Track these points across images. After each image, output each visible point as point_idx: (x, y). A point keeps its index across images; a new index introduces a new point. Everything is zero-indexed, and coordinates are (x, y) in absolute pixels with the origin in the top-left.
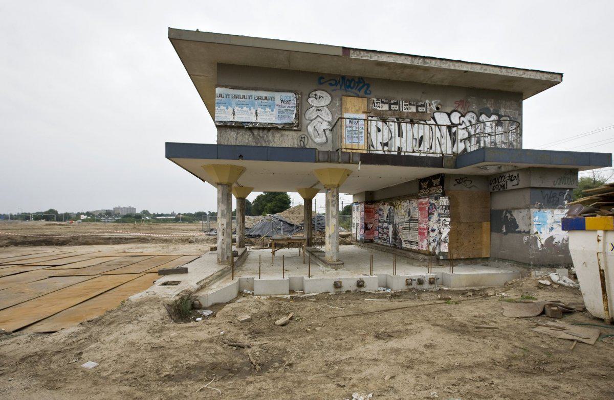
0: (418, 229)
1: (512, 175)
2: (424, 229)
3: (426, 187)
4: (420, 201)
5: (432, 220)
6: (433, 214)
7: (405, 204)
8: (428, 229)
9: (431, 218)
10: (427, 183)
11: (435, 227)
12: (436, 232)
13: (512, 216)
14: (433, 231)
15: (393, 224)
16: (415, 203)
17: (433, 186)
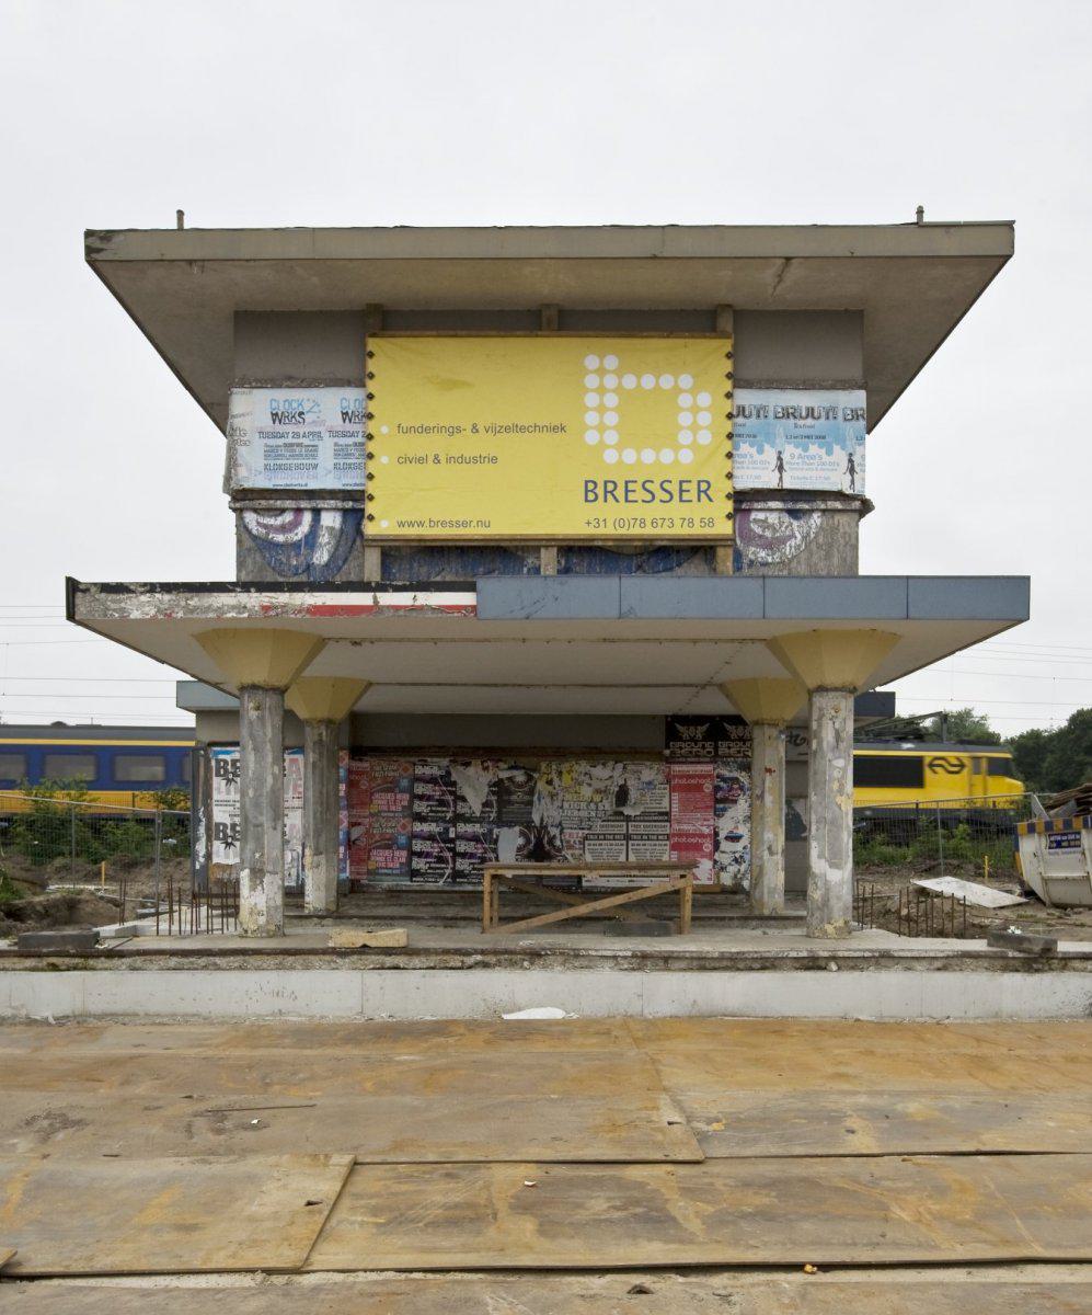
0: (668, 837)
1: (798, 736)
2: (702, 836)
3: (699, 736)
4: (677, 768)
5: (729, 814)
6: (735, 802)
7: (600, 772)
8: (716, 834)
9: (725, 810)
10: (705, 728)
11: (743, 830)
12: (745, 842)
13: (793, 809)
14: (734, 838)
15: (528, 824)
16: (650, 772)
17: (726, 737)
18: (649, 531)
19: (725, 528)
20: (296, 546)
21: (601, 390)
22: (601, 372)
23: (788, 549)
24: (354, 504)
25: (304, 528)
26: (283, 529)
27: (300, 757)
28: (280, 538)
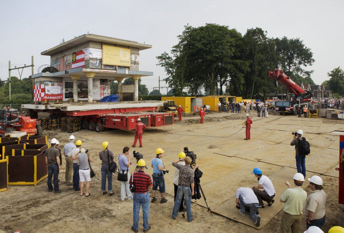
18: (123, 65)
19: (130, 66)
20: (95, 64)
21: (121, 53)
22: (121, 51)
23: (134, 68)
24: (101, 61)
25: (96, 62)
26: (94, 62)
27: (57, 83)
28: (93, 63)
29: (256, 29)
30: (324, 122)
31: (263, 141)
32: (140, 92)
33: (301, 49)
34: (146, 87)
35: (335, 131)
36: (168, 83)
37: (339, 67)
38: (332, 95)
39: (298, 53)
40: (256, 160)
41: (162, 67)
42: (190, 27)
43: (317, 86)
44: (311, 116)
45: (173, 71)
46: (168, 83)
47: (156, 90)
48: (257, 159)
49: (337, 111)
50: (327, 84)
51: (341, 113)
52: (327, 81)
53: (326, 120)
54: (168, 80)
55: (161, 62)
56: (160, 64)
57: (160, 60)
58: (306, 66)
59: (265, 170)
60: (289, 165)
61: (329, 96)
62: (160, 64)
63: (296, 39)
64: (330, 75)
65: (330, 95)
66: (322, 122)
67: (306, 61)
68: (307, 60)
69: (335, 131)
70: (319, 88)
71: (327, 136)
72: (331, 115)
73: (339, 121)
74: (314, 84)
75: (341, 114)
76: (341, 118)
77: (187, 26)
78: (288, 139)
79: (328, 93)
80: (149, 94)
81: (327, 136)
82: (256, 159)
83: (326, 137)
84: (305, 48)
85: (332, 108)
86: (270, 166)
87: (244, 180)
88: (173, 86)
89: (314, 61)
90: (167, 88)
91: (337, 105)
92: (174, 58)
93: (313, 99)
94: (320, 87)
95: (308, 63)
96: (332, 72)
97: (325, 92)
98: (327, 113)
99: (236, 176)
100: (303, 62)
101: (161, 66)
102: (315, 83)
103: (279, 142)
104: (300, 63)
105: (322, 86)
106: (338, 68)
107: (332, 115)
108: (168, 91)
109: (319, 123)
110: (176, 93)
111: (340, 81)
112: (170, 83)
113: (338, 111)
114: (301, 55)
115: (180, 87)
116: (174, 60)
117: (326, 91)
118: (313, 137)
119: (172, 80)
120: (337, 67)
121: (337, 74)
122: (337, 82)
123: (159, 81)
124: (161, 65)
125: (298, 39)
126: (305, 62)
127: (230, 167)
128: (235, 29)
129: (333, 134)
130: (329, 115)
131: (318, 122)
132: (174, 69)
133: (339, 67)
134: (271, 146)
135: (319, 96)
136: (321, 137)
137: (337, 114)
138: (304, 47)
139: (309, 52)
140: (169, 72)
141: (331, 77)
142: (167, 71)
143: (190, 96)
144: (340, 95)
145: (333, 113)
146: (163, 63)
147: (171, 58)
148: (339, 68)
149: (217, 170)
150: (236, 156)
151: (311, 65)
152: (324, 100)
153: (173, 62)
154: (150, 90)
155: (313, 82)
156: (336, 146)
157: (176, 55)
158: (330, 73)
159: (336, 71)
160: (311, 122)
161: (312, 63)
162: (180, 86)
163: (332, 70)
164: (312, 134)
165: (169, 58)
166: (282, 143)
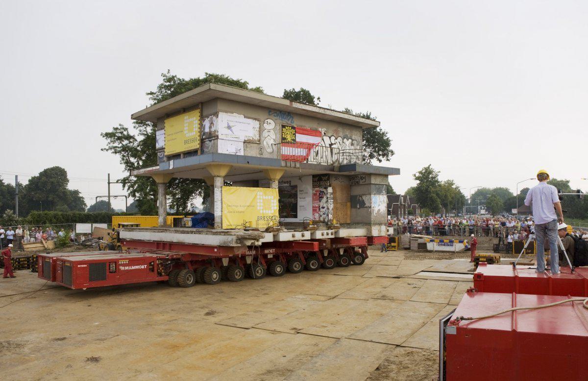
29: (300, 92)
30: (407, 258)
31: (306, 296)
32: (68, 206)
33: (374, 132)
34: (81, 195)
35: (422, 271)
36: (126, 188)
37: (430, 165)
38: (420, 211)
39: (368, 138)
40: (293, 332)
41: (114, 155)
42: (173, 77)
43: (399, 196)
44: (388, 248)
45: (138, 164)
46: (126, 188)
47: (102, 201)
48: (295, 329)
49: (426, 238)
50: (413, 192)
51: (432, 241)
52: (413, 189)
53: (409, 254)
54: (127, 181)
55: (112, 145)
56: (111, 148)
57: (109, 140)
58: (380, 161)
59: (308, 347)
60: (349, 334)
61: (415, 213)
62: (111, 148)
63: (365, 114)
64: (417, 179)
65: (418, 211)
66: (404, 258)
67: (381, 153)
68: (383, 151)
69: (422, 271)
70: (401, 200)
71: (410, 281)
72: (416, 245)
73: (428, 254)
74: (394, 193)
75: (431, 243)
76: (432, 249)
77: (168, 75)
78: (349, 290)
79: (414, 208)
80: (87, 209)
81: (410, 281)
82: (292, 329)
83: (407, 282)
84: (379, 131)
85: (420, 233)
86: (315, 340)
87: (270, 369)
88: (137, 195)
89: (392, 152)
90: (126, 197)
91: (427, 230)
92: (140, 138)
93: (391, 217)
94: (402, 198)
95: (383, 155)
96: (420, 173)
97: (409, 206)
98: (412, 242)
99: (256, 363)
100: (375, 154)
101: (113, 152)
102: (394, 191)
103: (332, 294)
104: (371, 156)
105: (405, 197)
106: (429, 167)
107: (419, 244)
108: (128, 205)
109: (398, 258)
110: (143, 208)
111: (431, 188)
112: (131, 189)
113: (427, 238)
114: (373, 143)
115: (152, 197)
116: (140, 142)
117: (411, 203)
118: (389, 283)
119: (135, 182)
120: (427, 166)
121: (427, 177)
122: (427, 190)
123: (109, 183)
124: (113, 150)
125: (369, 114)
126: (380, 155)
127: (244, 349)
128: (261, 89)
129: (419, 276)
130: (414, 246)
131: (396, 258)
132: (141, 159)
133: (430, 165)
134: (320, 303)
135: (401, 213)
136: (401, 282)
137: (426, 244)
138: (378, 129)
139: (385, 138)
140: (130, 166)
141: (418, 182)
142: (125, 163)
143: (173, 214)
144: (431, 212)
145: (420, 241)
146: (116, 147)
147: (132, 137)
148: (429, 166)
149: (221, 355)
150: (256, 327)
151: (388, 160)
152: (406, 221)
153: (138, 146)
154: (90, 202)
155: (392, 190)
156: (421, 296)
157: (145, 133)
158: (417, 175)
159: (426, 172)
160: (386, 258)
161: (390, 157)
162: (151, 195)
163: (420, 170)
164: (387, 279)
165: (129, 137)
166: (338, 297)
